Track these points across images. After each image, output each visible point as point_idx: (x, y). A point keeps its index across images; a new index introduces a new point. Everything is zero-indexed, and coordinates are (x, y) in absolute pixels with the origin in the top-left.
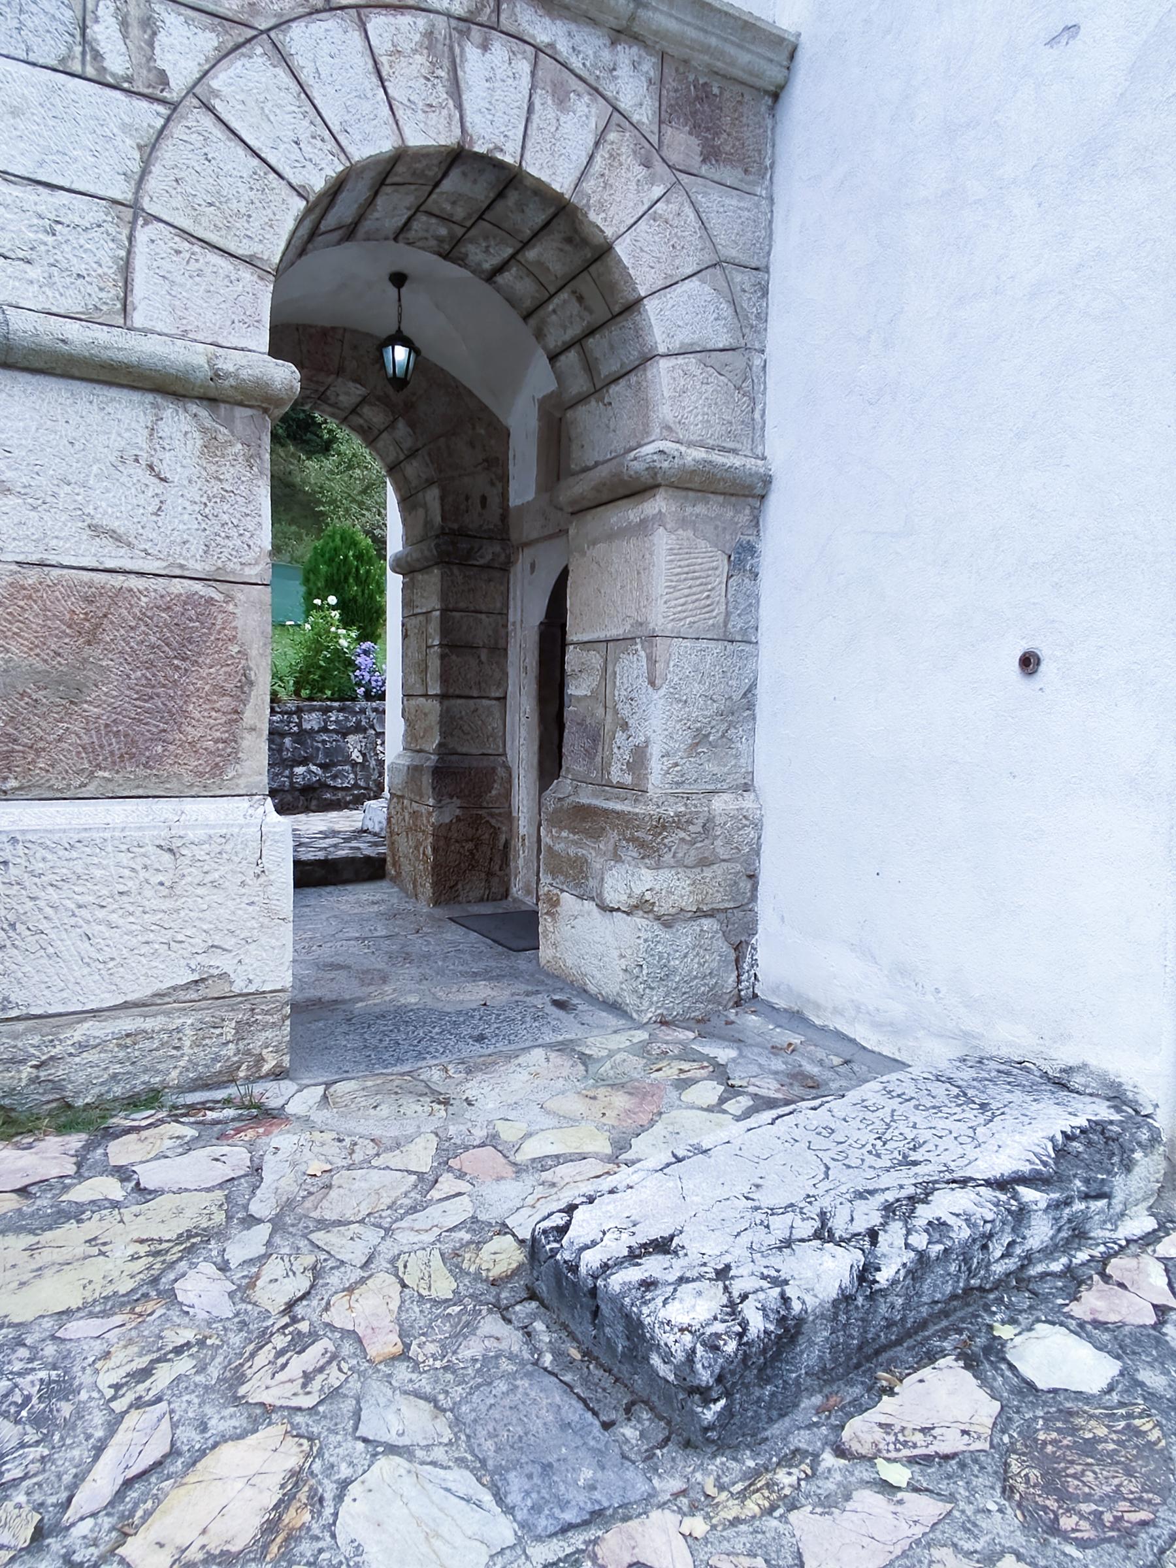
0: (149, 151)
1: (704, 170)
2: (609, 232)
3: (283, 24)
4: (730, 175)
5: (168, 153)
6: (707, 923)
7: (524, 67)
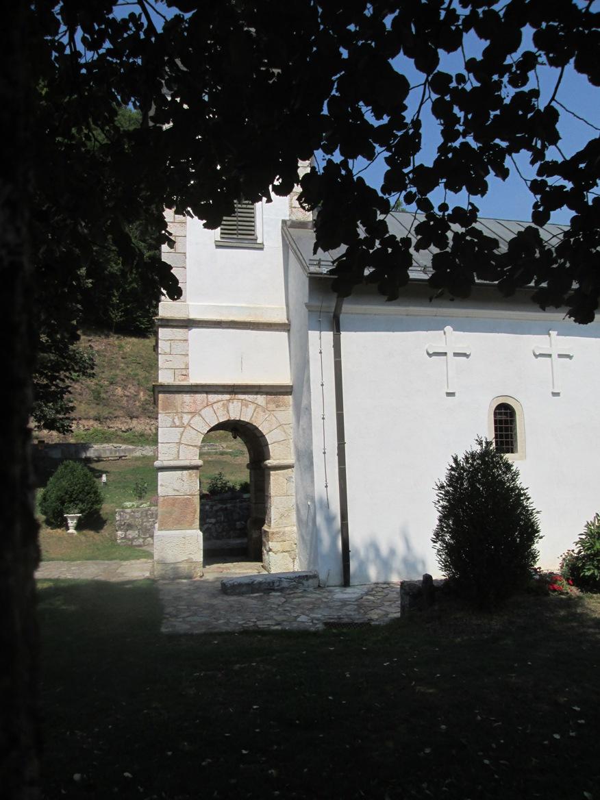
0: (182, 435)
1: (277, 409)
2: (257, 426)
3: (200, 410)
4: (282, 409)
5: (184, 434)
6: (286, 554)
7: (240, 404)
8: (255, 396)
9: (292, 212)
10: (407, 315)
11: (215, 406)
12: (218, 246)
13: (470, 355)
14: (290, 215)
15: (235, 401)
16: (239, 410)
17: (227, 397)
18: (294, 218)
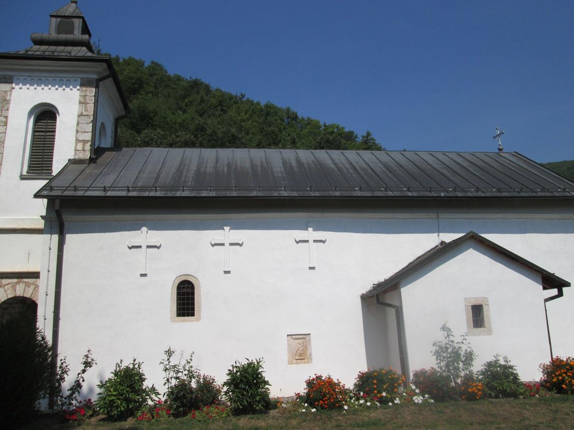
8: (36, 280)
9: (75, 154)
10: (115, 221)
11: (6, 287)
12: (23, 178)
13: (160, 246)
14: (74, 156)
15: (21, 284)
16: (21, 289)
17: (15, 280)
18: (77, 157)
